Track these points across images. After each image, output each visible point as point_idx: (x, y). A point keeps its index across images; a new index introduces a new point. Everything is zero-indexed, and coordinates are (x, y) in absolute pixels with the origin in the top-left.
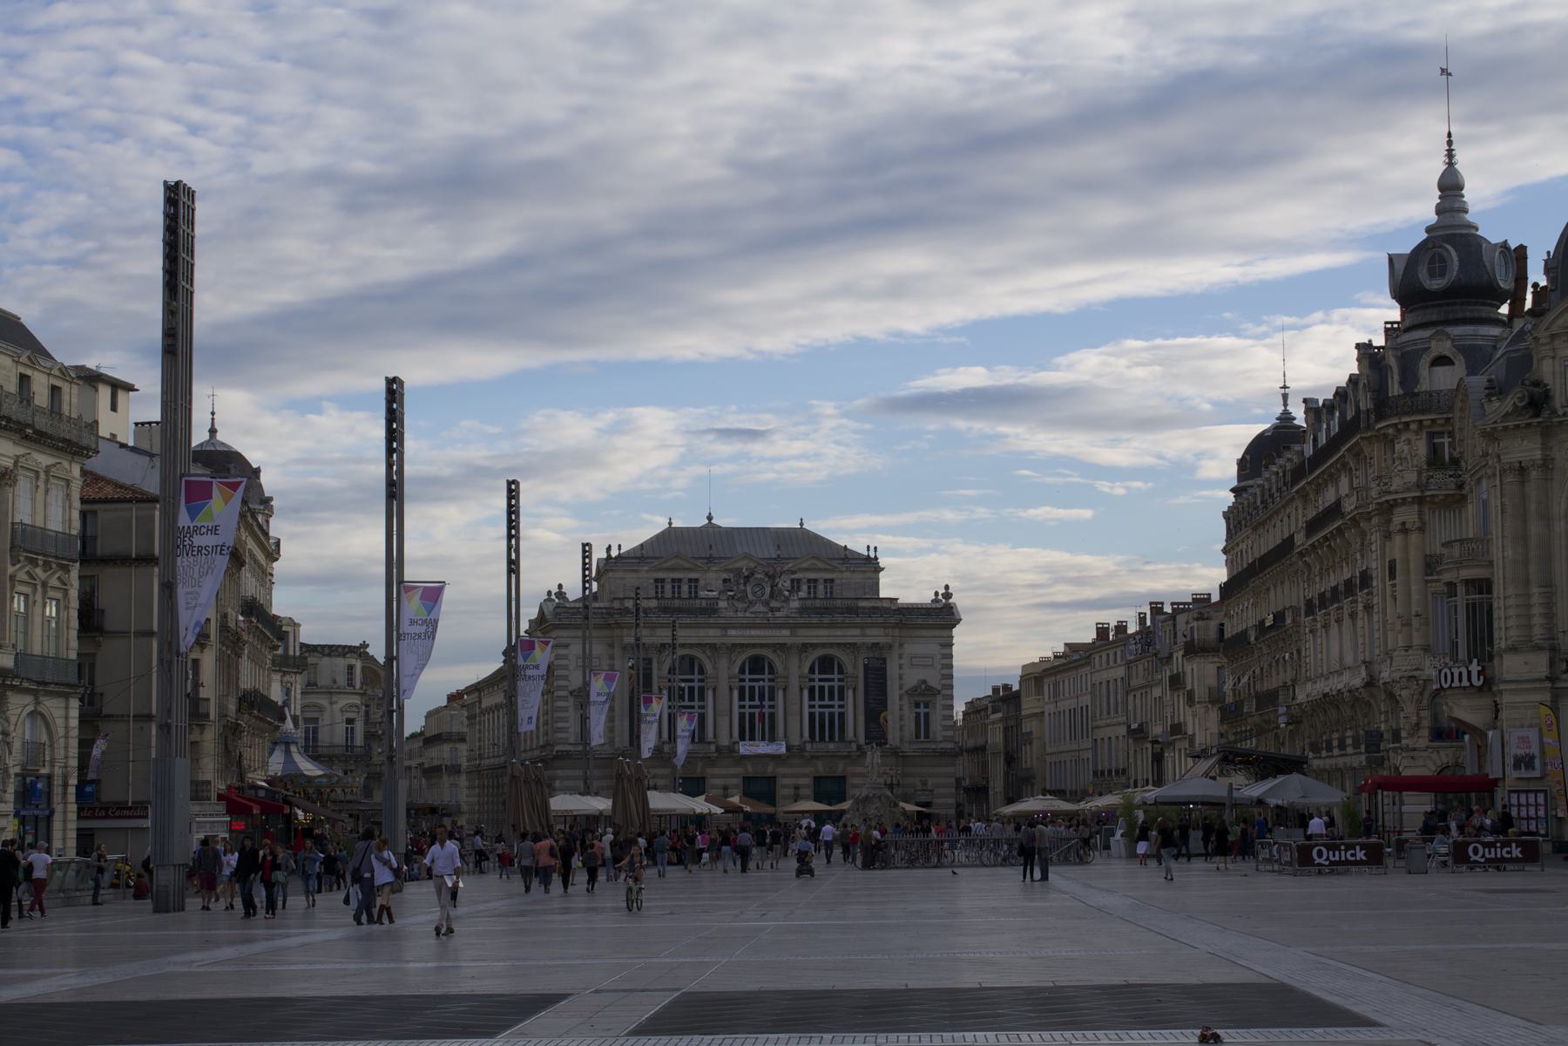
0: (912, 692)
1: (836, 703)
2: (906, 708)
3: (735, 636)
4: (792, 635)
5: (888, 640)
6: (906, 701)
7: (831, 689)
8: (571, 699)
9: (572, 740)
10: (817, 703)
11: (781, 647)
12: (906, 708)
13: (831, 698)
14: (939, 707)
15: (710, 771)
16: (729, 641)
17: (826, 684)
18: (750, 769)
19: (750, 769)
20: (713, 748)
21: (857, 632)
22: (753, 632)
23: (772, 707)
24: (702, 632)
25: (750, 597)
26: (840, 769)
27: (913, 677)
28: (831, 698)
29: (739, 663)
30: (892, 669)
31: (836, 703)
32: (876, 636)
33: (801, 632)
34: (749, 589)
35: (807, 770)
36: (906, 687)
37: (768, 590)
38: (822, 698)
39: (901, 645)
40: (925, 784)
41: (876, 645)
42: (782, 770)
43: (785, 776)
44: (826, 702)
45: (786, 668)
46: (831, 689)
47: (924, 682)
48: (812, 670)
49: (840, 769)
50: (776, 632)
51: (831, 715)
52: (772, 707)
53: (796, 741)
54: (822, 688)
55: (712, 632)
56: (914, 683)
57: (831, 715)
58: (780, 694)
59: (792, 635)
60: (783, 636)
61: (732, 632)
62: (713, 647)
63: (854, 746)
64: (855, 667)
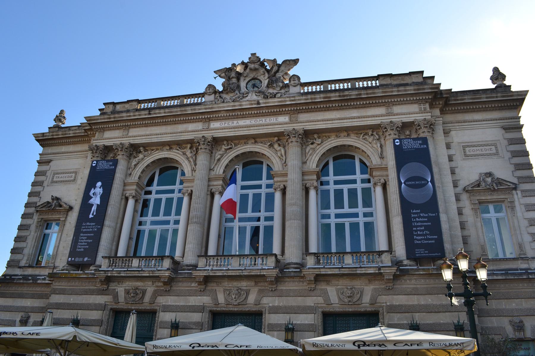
0: (472, 190)
1: (360, 210)
2: (468, 211)
3: (220, 128)
4: (291, 122)
5: (428, 116)
6: (466, 202)
7: (353, 193)
8: (36, 217)
9: (23, 263)
10: (333, 211)
11: (279, 138)
12: (468, 211)
13: (353, 204)
14: (519, 210)
15: (162, 300)
16: (209, 135)
17: (345, 188)
18: (221, 298)
19: (221, 298)
20: (167, 263)
21: (381, 110)
22: (242, 122)
23: (267, 219)
24: (181, 127)
25: (243, 89)
26: (367, 299)
27: (471, 171)
28: (353, 204)
29: (225, 161)
30: (438, 152)
31: (360, 210)
32: (409, 112)
33: (303, 117)
34: (243, 84)
35: (310, 301)
36: (463, 184)
37: (265, 82)
38: (339, 204)
39: (446, 133)
40: (520, 327)
41: (405, 126)
42: (268, 301)
43: (275, 310)
44: (346, 210)
45: (285, 164)
46: (353, 193)
47: (490, 174)
48: (324, 170)
49: (367, 299)
50: (272, 120)
51: (355, 227)
52: (267, 219)
53: (292, 255)
54: (339, 194)
55: (191, 127)
56: (474, 177)
57: (355, 227)
58: (278, 196)
59: (291, 122)
60: (280, 123)
61: (215, 125)
62: (193, 145)
63: (386, 259)
64: (381, 154)
